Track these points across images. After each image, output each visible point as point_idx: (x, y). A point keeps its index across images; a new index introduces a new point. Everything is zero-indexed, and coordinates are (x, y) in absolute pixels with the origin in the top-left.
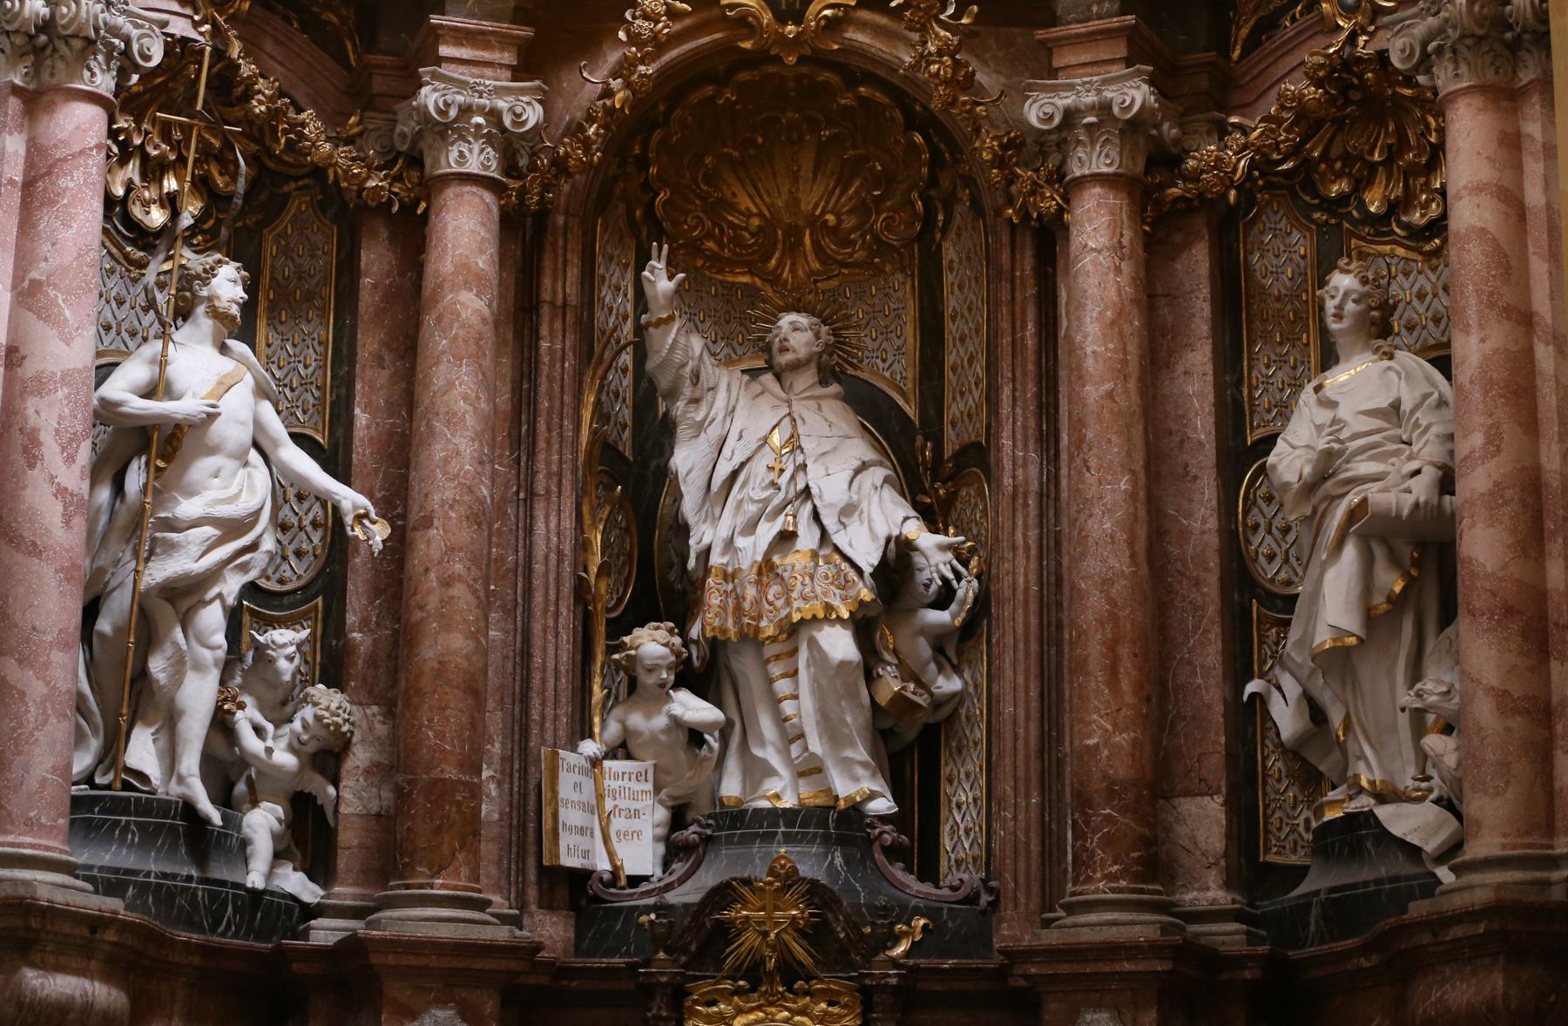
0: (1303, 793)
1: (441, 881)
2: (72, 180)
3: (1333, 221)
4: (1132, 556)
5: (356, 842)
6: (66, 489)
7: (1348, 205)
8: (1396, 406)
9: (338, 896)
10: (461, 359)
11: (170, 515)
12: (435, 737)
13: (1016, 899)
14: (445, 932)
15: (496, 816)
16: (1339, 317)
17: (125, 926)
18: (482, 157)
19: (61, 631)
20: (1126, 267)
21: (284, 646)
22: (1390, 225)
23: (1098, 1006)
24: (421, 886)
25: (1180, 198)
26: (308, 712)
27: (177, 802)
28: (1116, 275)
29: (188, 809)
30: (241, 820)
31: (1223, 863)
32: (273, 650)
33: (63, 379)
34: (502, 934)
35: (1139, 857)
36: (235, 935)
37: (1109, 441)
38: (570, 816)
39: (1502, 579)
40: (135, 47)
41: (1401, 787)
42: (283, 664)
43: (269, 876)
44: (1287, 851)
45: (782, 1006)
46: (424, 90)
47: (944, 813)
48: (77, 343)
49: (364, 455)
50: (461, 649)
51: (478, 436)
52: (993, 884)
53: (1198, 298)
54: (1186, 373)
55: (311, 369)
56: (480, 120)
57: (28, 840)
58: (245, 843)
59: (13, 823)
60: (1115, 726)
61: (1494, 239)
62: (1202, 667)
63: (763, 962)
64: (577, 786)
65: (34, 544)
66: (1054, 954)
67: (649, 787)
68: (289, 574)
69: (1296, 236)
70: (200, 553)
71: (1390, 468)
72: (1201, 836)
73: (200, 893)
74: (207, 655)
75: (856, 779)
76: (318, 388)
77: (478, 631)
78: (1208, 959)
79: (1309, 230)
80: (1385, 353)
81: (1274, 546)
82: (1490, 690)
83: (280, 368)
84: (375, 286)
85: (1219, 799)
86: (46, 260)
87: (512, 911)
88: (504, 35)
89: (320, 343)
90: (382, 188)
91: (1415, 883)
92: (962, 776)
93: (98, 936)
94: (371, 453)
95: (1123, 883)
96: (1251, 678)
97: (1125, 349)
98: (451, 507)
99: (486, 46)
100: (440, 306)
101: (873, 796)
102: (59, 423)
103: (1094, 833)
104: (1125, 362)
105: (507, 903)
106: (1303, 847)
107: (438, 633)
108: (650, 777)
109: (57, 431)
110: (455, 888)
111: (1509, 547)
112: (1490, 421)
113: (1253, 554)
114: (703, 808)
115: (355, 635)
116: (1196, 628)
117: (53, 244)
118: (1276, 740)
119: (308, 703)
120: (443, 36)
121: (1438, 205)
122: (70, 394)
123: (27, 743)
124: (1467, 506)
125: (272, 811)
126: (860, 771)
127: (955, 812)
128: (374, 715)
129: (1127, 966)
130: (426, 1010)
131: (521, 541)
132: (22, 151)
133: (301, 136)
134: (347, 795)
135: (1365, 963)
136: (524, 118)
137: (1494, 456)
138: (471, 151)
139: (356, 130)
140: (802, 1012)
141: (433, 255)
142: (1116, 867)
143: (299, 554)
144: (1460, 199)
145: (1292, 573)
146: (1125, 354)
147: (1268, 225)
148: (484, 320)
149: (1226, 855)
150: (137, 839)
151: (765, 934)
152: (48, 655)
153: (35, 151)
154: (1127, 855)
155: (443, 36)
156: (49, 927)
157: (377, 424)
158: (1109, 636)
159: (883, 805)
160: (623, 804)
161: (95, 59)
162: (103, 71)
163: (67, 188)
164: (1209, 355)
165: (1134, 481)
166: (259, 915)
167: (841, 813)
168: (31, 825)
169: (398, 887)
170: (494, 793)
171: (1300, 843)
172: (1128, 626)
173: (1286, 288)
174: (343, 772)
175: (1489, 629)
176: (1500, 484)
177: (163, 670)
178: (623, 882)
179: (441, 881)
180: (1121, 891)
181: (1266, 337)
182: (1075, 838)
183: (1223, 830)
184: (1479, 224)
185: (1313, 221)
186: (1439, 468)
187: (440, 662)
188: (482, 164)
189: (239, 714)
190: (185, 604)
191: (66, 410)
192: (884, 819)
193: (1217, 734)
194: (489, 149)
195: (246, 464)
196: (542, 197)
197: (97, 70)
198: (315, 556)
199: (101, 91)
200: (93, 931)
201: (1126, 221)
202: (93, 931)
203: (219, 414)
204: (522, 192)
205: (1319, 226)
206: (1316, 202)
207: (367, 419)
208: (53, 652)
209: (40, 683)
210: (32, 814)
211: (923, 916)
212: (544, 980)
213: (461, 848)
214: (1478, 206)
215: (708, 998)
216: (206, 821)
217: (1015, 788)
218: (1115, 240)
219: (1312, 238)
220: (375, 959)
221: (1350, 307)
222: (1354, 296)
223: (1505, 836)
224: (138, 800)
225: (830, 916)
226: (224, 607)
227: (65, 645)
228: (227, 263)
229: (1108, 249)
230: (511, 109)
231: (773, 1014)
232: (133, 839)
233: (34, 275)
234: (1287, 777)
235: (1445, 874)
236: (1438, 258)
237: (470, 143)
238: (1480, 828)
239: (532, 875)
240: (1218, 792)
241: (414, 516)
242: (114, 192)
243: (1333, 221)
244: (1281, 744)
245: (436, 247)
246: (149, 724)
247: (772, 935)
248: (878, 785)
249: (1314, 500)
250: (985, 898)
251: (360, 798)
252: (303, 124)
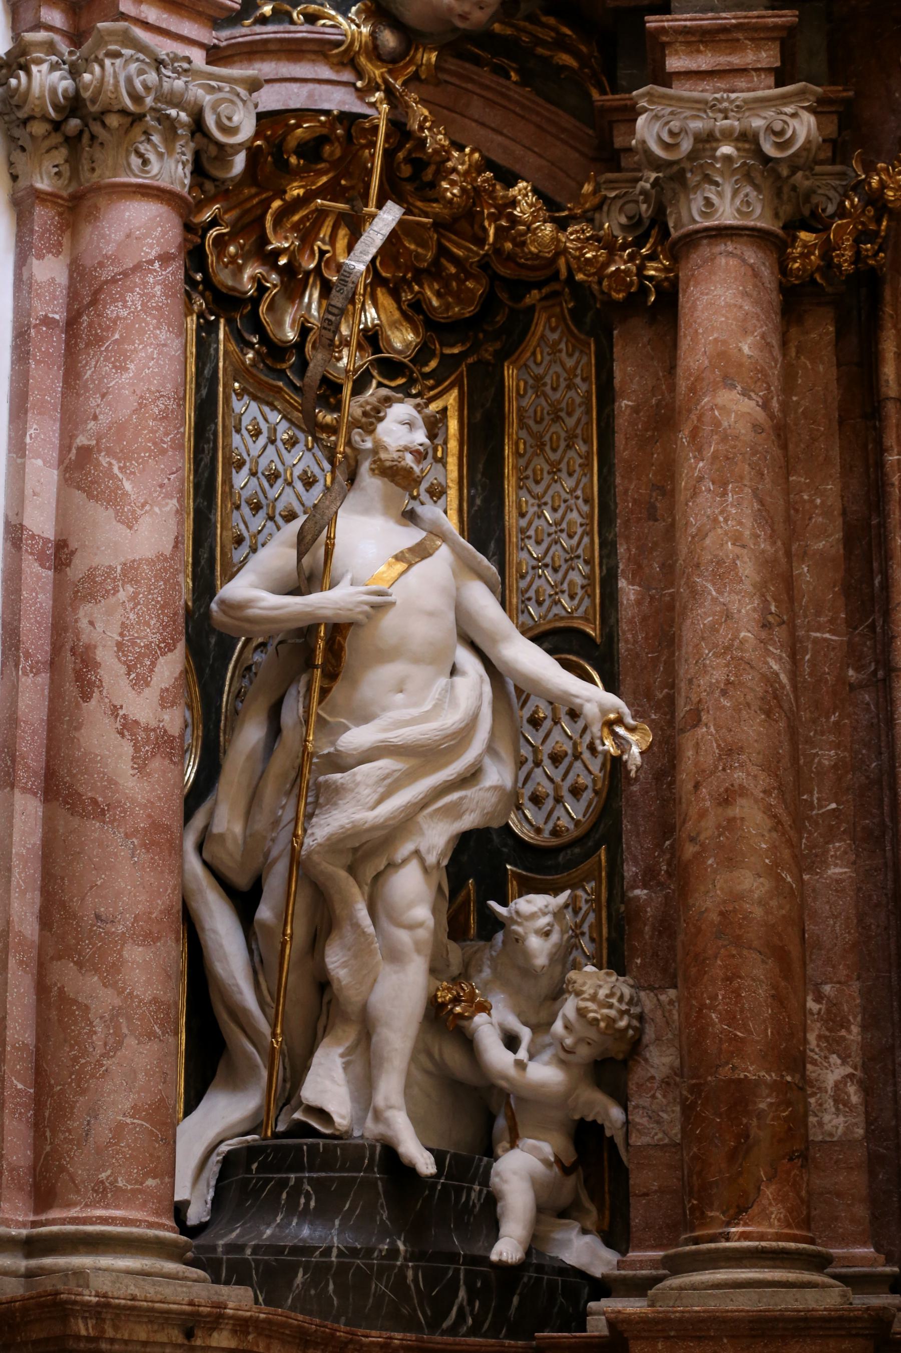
1: (740, 1229)
2: (125, 306)
5: (655, 1186)
6: (136, 722)
9: (632, 1265)
10: (725, 484)
11: (332, 750)
12: (721, 1021)
15: (860, 1132)
17: (242, 1326)
18: (738, 202)
19: (136, 919)
21: (533, 916)
24: (713, 1239)
26: (569, 1007)
27: (372, 1148)
30: (489, 1167)
32: (519, 924)
33: (124, 572)
36: (474, 1331)
40: (210, 121)
42: (535, 942)
46: (641, 120)
48: (145, 525)
49: (635, 642)
50: (751, 891)
51: (761, 588)
55: (576, 538)
56: (726, 149)
59: (78, 1192)
65: (94, 802)
68: (564, 822)
70: (375, 797)
73: (410, 1273)
74: (404, 937)
76: (586, 562)
77: (776, 864)
83: (538, 543)
84: (636, 410)
86: (95, 418)
87: (888, 1269)
88: (755, 28)
89: (586, 501)
90: (627, 272)
93: (199, 1342)
94: (646, 638)
98: (724, 693)
99: (734, 46)
100: (693, 417)
102: (121, 635)
105: (882, 1258)
107: (715, 871)
109: (119, 645)
110: (762, 1237)
115: (638, 892)
117: (103, 396)
119: (570, 993)
120: (669, 44)
122: (136, 594)
123: (93, 1076)
125: (533, 1151)
128: (671, 1002)
131: (883, 738)
132: (62, 278)
133: (514, 221)
136: (789, 133)
138: (720, 195)
139: (596, 200)
141: (684, 344)
143: (576, 791)
148: (757, 428)
150: (313, 1204)
152: (120, 952)
153: (77, 270)
155: (669, 44)
157: (652, 598)
161: (149, 140)
162: (160, 155)
163: (118, 318)
166: (516, 1300)
169: (687, 1242)
170: (855, 1099)
174: (632, 1086)
177: (344, 965)
179: (740, 1229)
187: (722, 914)
188: (739, 211)
189: (480, 1019)
190: (369, 873)
191: (132, 616)
194: (748, 189)
195: (454, 671)
196: (858, 253)
197: (152, 156)
198: (596, 792)
199: (164, 183)
200: (189, 1334)
202: (189, 1334)
203: (393, 604)
204: (828, 249)
207: (637, 593)
208: (128, 947)
209: (110, 991)
210: (103, 1176)
213: (769, 1180)
216: (410, 1171)
224: (313, 1148)
226: (426, 870)
227: (146, 937)
228: (401, 401)
230: (770, 129)
232: (307, 1204)
233: (81, 440)
237: (717, 184)
241: (682, 709)
242: (280, 336)
245: (685, 336)
246: (338, 1043)
252: (514, 203)
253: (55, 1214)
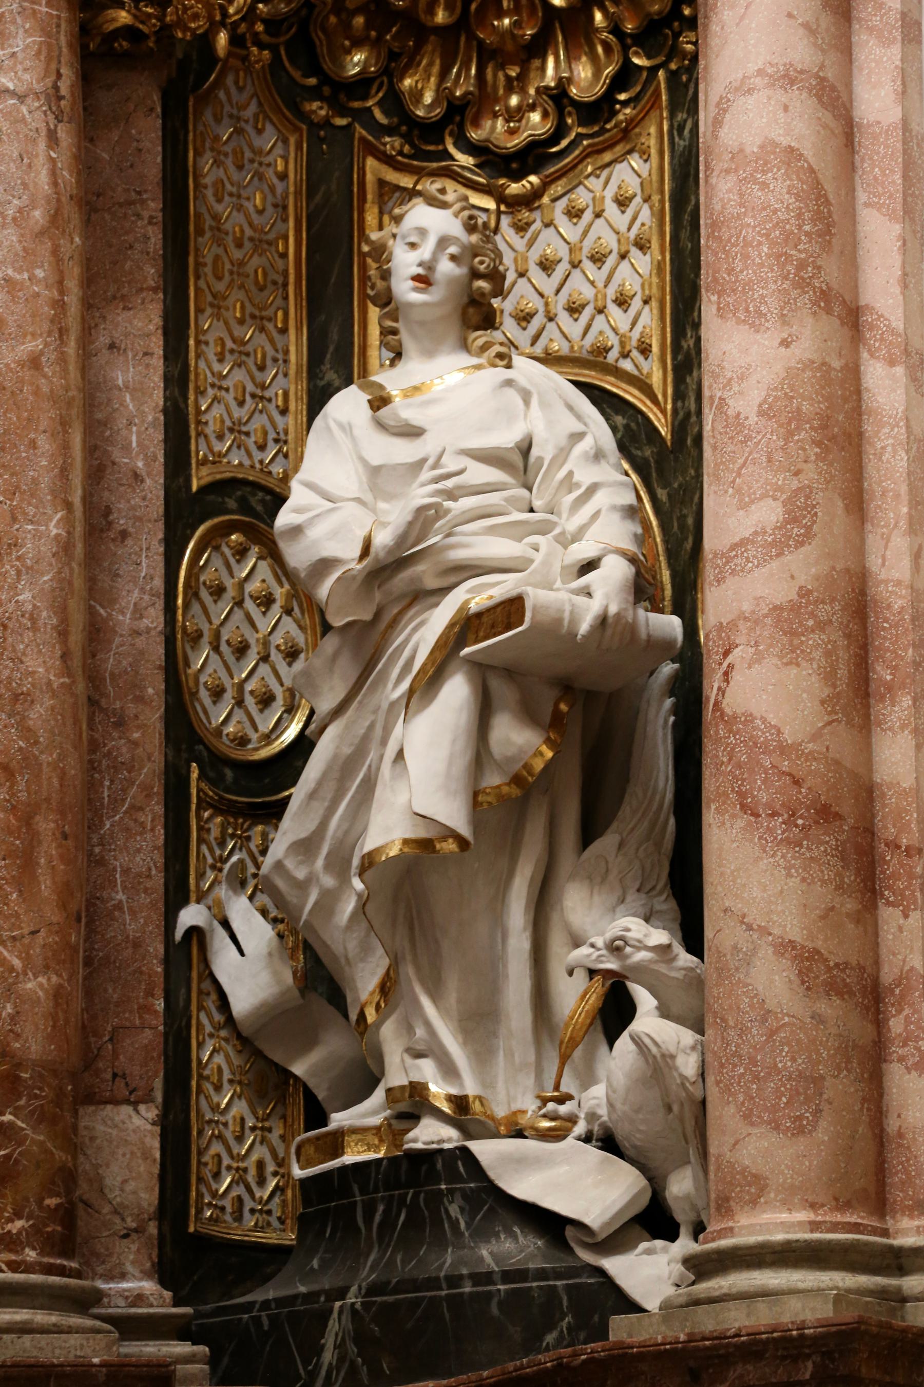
0: (254, 1113)
3: (341, 122)
4: (65, 656)
7: (365, 98)
8: (525, 448)
16: (423, 280)
20: (64, 133)
22: (442, 141)
25: (129, 32)
28: (50, 147)
31: (153, 1229)
35: (58, 1206)
37: (33, 444)
39: (811, 756)
41: (500, 1112)
44: (228, 1218)
53: (139, 216)
54: (112, 346)
60: (27, 960)
61: (812, 170)
62: (126, 871)
69: (269, 139)
71: (531, 553)
72: (113, 1176)
79: (297, 129)
80: (500, 356)
81: (223, 674)
82: (785, 947)
85: (150, 1112)
91: (559, 1283)
95: (31, 1255)
96: (185, 902)
97: (60, 282)
104: (60, 305)
106: (252, 1211)
111: (823, 702)
112: (795, 484)
113: (191, 684)
116: (116, 802)
118: (218, 1017)
121: (545, 115)
124: (742, 625)
137: (802, 544)
142: (19, 1224)
144: (750, 91)
145: (247, 724)
146: (62, 292)
147: (227, 108)
154: (40, 1202)
158: (23, 796)
164: (158, 321)
165: (67, 521)
171: (249, 1204)
172: (56, 782)
173: (251, 225)
175: (787, 842)
176: (809, 592)
180: (28, 1268)
181: (218, 304)
183: (156, 1170)
184: (785, 141)
185: (304, 116)
186: (633, 560)
193: (150, 993)
201: (65, 50)
205: (313, 126)
206: (313, 81)
214: (786, 108)
218: (49, 82)
219: (299, 147)
221: (446, 267)
222: (453, 250)
223: (813, 1206)
229: (37, 96)
234: (231, 1081)
236: (531, 210)
238: (762, 1190)
240: (147, 1099)
243: (341, 122)
244: (230, 1019)
249: (378, 596)
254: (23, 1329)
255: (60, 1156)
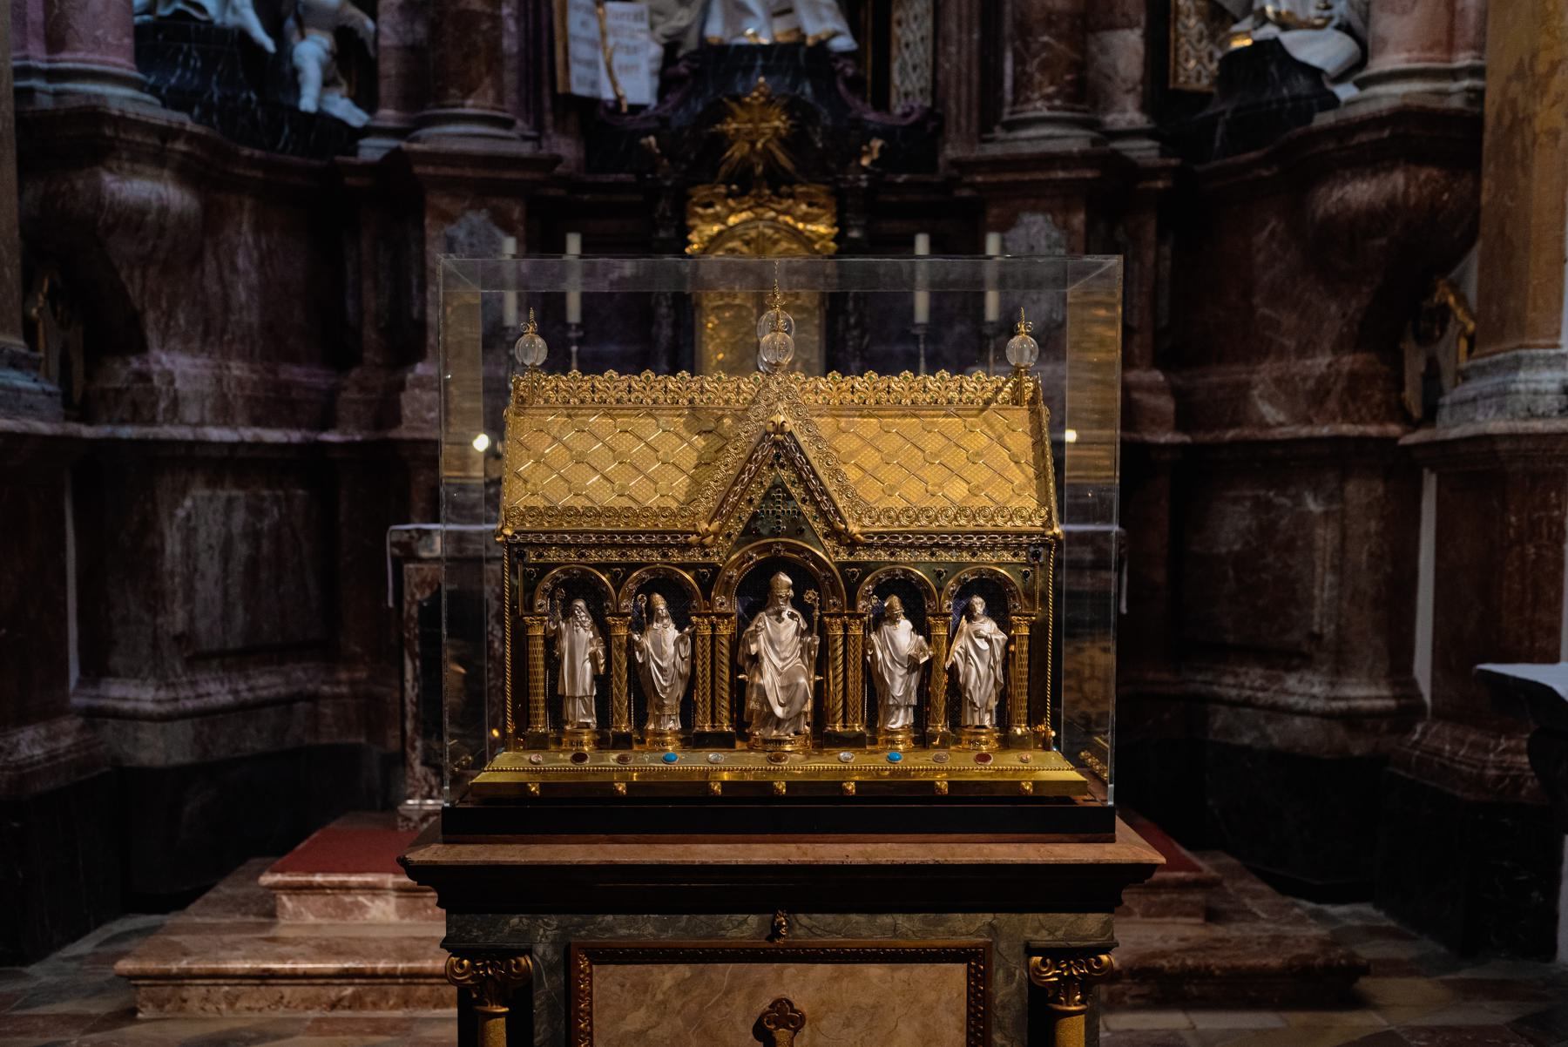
13: (958, 123)
14: (475, 147)
17: (192, 138)
23: (1034, 210)
29: (244, 35)
31: (1140, 88)
34: (526, 149)
35: (1072, 81)
38: (580, 50)
43: (320, 101)
45: (768, 207)
47: (894, 51)
52: (938, 110)
57: (97, 57)
58: (296, 72)
63: (751, 168)
64: (584, 24)
66: (997, 164)
67: (645, 26)
75: (821, 19)
78: (1130, 170)
92: (911, 20)
93: (169, 145)
101: (835, 34)
103: (1035, 56)
108: (646, 16)
114: (691, 42)
125: (319, 43)
126: (825, 12)
127: (904, 50)
129: (1061, 174)
130: (463, 215)
134: (385, 29)
135: (1265, 173)
140: (786, 213)
149: (1143, 81)
151: (753, 144)
156: (122, 135)
159: (844, 43)
160: (625, 41)
166: (312, 136)
167: (810, 49)
168: (97, 43)
178: (625, 109)
182: (1015, 63)
192: (845, 55)
200: (164, 141)
202: (164, 141)
211: (880, 137)
212: (561, 192)
215: (706, 200)
216: (260, 48)
217: (959, 26)
220: (417, 169)
223: (1409, 51)
225: (810, 128)
231: (762, 215)
235: (1345, 92)
239: (547, 104)
240: (1138, 25)
247: (759, 145)
248: (839, 24)
250: (930, 126)
251: (397, 32)
253: (65, 55)
254: (1050, 137)
255: (1077, 56)
